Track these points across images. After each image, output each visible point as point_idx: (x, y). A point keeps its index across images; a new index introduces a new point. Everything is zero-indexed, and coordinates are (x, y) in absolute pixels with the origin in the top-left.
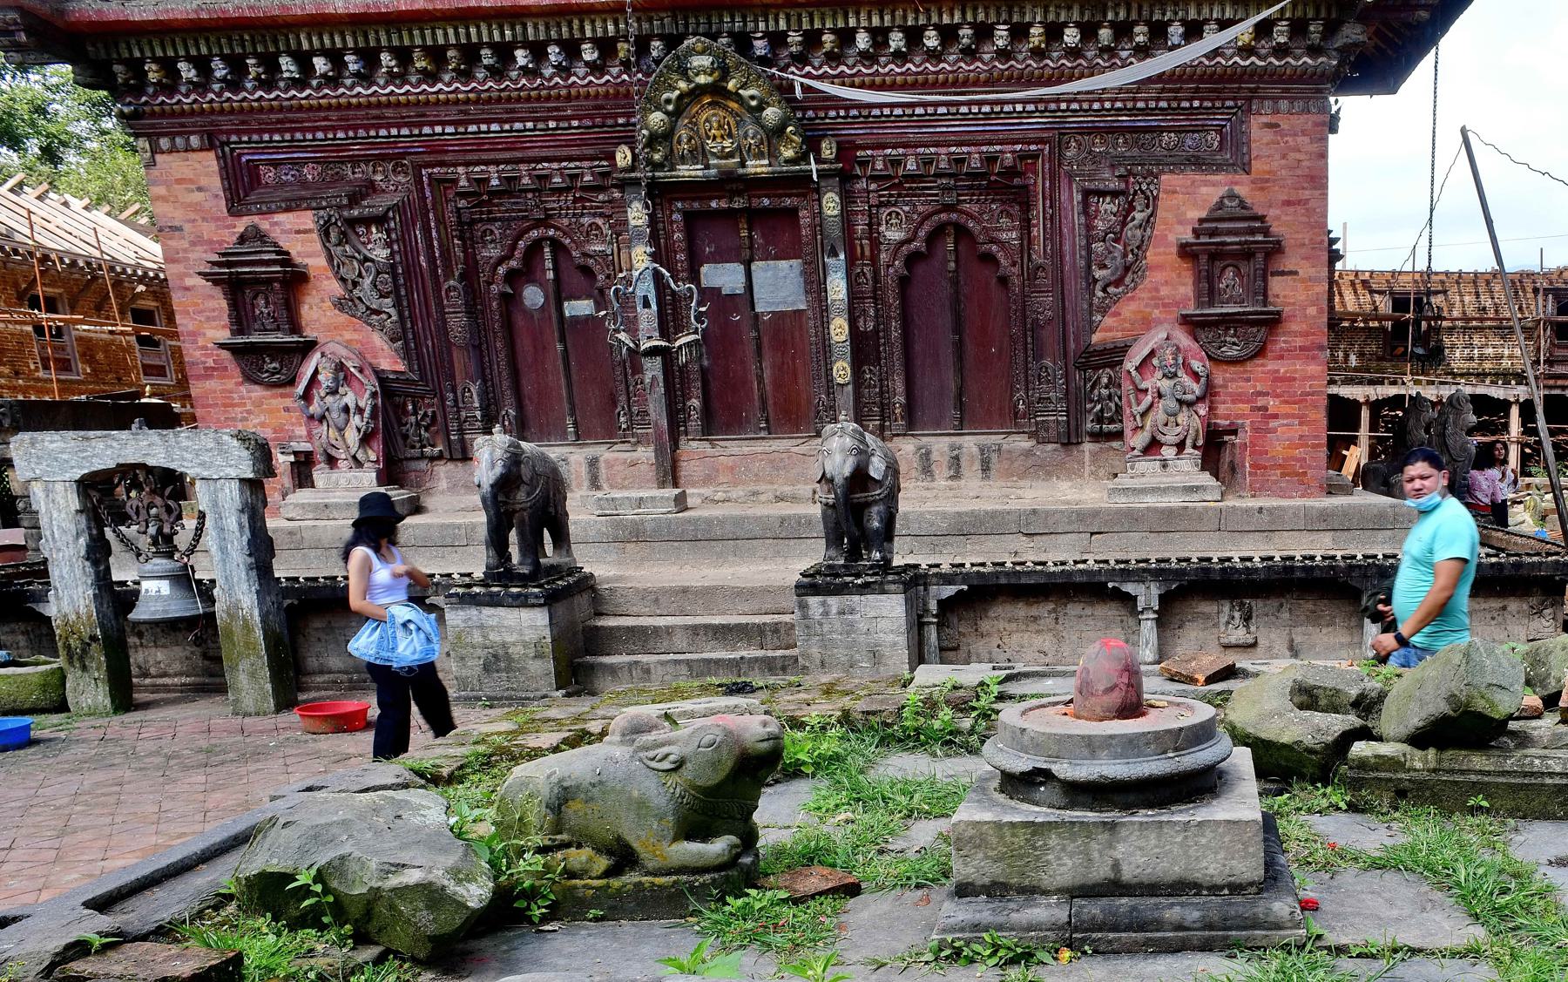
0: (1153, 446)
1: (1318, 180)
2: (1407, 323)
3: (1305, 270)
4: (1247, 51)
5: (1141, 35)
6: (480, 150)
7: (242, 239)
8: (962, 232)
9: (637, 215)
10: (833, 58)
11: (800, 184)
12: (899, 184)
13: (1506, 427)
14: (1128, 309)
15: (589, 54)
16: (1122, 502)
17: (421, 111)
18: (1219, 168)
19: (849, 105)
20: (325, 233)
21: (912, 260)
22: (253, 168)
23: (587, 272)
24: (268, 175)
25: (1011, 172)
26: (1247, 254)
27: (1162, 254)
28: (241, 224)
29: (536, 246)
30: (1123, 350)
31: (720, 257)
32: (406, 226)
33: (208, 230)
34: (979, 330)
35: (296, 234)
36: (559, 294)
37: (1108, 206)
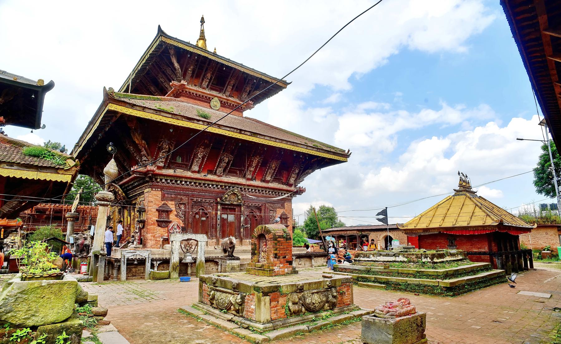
7: (163, 204)
17: (194, 190)
20: (176, 205)
28: (163, 202)
31: (224, 214)
33: (157, 203)
35: (171, 205)
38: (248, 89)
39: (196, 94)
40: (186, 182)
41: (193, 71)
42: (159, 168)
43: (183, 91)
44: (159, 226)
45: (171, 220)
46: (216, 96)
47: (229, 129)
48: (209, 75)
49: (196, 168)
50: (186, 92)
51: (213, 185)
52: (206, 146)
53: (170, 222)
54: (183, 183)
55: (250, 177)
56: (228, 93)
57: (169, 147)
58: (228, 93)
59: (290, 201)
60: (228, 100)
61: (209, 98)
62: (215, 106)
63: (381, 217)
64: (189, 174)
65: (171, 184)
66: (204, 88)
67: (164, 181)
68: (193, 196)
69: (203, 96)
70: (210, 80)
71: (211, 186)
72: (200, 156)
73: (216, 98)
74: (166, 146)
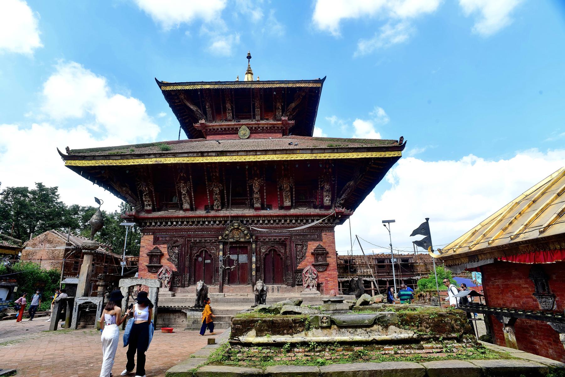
0: (308, 286)
1: (334, 242)
2: (347, 265)
3: (332, 256)
4: (321, 223)
5: (304, 221)
6: (197, 236)
8: (275, 251)
9: (221, 247)
10: (256, 224)
11: (249, 243)
12: (265, 243)
14: (303, 263)
15: (217, 223)
16: (303, 296)
17: (189, 230)
18: (317, 241)
19: (258, 231)
20: (168, 248)
21: (266, 255)
22: (158, 238)
23: (210, 256)
24: (161, 239)
25: (283, 241)
26: (323, 254)
27: (308, 254)
29: (202, 251)
32: (182, 247)
33: (149, 247)
34: (279, 267)
35: (163, 248)
36: (205, 259)
37: (299, 247)
39: (221, 129)
41: (211, 106)
42: (149, 212)
43: (207, 130)
44: (149, 271)
45: (162, 264)
46: (243, 125)
47: (186, 155)
48: (228, 106)
49: (186, 206)
50: (210, 130)
52: (186, 180)
53: (162, 266)
55: (258, 205)
57: (149, 189)
58: (258, 117)
59: (331, 229)
60: (259, 124)
61: (237, 128)
62: (244, 135)
63: (420, 237)
64: (181, 213)
67: (153, 224)
68: (189, 236)
69: (229, 129)
70: (232, 109)
73: (244, 127)
74: (145, 188)
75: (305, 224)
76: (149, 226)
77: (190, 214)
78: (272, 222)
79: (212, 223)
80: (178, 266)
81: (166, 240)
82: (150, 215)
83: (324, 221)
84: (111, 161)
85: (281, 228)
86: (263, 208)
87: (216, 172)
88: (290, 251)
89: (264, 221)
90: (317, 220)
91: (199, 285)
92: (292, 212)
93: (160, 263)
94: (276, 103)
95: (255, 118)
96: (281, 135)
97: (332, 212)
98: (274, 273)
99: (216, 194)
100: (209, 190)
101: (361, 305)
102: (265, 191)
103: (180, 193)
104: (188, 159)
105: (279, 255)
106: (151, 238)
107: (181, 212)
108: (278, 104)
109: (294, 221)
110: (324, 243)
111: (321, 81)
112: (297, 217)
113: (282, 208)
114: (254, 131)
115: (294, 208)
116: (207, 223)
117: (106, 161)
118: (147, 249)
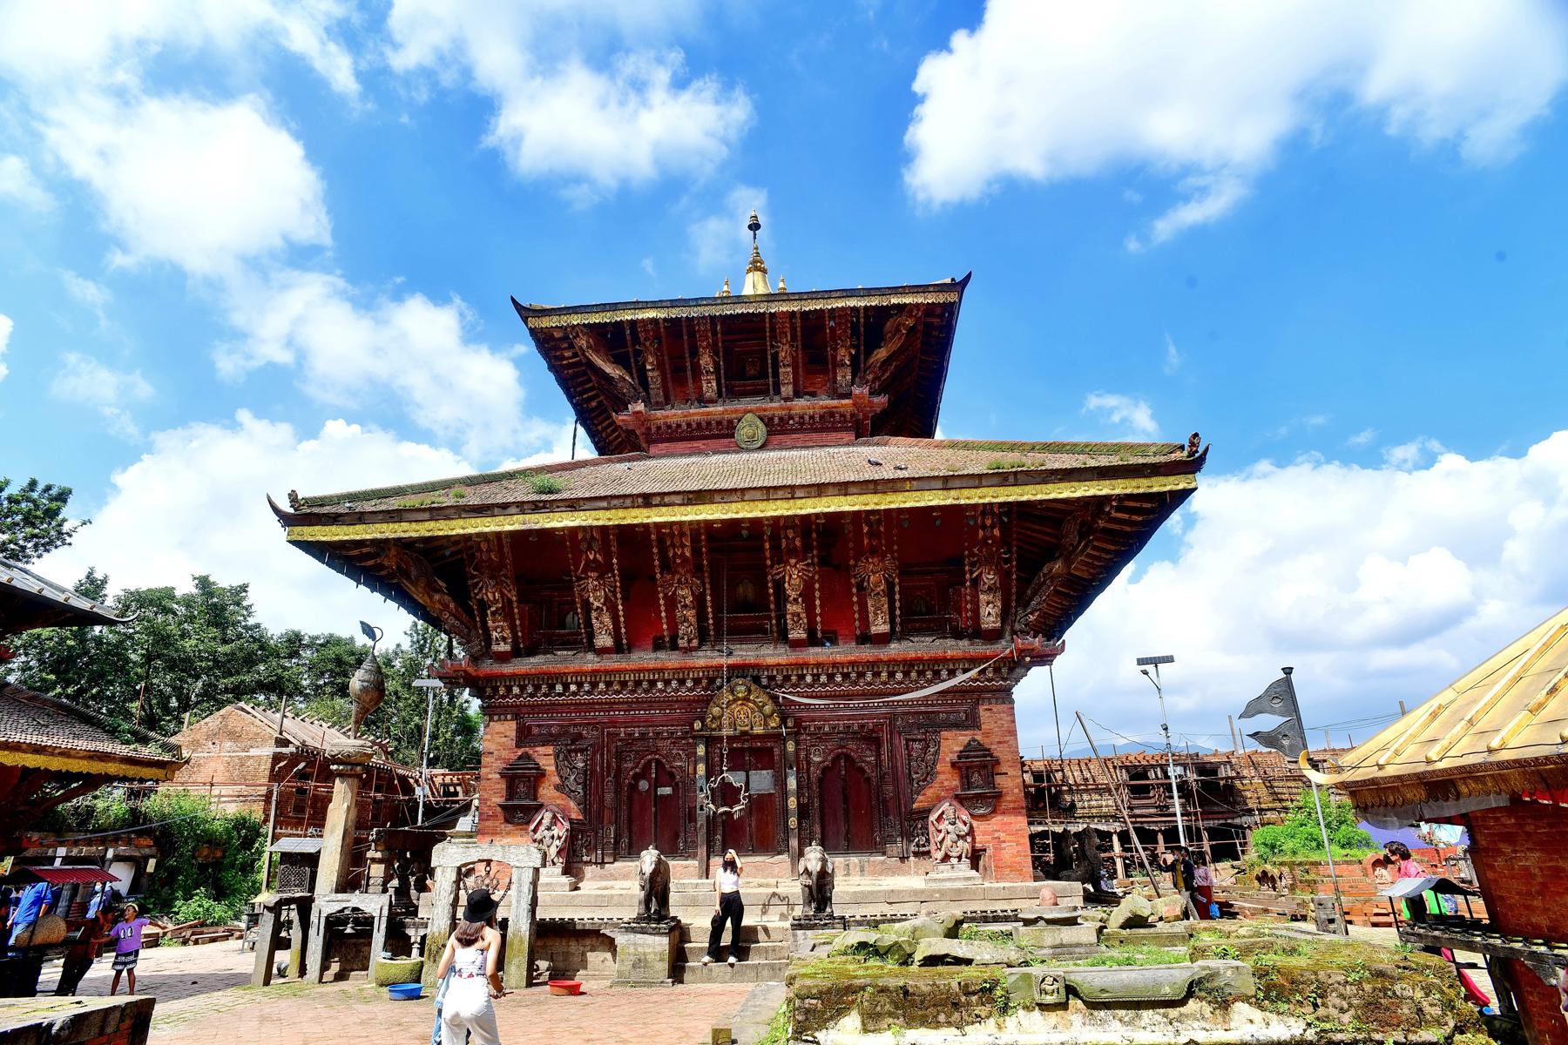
1: (1013, 733)
3: (1011, 772)
4: (971, 680)
5: (929, 675)
6: (633, 723)
7: (520, 758)
8: (848, 757)
9: (701, 750)
10: (794, 686)
11: (777, 737)
12: (819, 737)
13: (1111, 848)
14: (930, 792)
15: (689, 684)
16: (934, 886)
18: (967, 728)
19: (800, 704)
20: (557, 756)
21: (825, 770)
22: (530, 727)
23: (672, 775)
24: (535, 731)
25: (872, 731)
27: (943, 767)
29: (650, 762)
30: (929, 811)
32: (594, 753)
33: (505, 754)
34: (861, 804)
35: (545, 757)
36: (658, 783)
37: (917, 745)
38: (844, 355)
39: (689, 425)
40: (580, 685)
41: (660, 366)
42: (503, 658)
44: (507, 821)
47: (605, 504)
48: (706, 361)
49: (604, 640)
51: (667, 683)
52: (603, 570)
53: (541, 806)
54: (573, 688)
55: (798, 634)
56: (787, 390)
57: (502, 595)
58: (787, 390)
59: (1005, 695)
61: (730, 422)
62: (752, 439)
63: (1269, 722)
64: (590, 662)
65: (540, 699)
66: (712, 401)
67: (516, 690)
68: (613, 723)
69: (709, 423)
71: (660, 685)
72: (596, 604)
75: (930, 682)
76: (503, 697)
77: (612, 662)
78: (839, 679)
79: (674, 684)
80: (585, 804)
81: (551, 735)
82: (507, 669)
83: (983, 672)
84: (405, 525)
85: (864, 695)
86: (813, 640)
87: (683, 546)
88: (892, 758)
89: (816, 677)
90: (965, 671)
91: (649, 858)
92: (895, 649)
93: (535, 799)
94: (835, 349)
95: (778, 392)
96: (850, 436)
97: (1004, 648)
98: (847, 820)
99: (685, 606)
100: (666, 595)
101: (1123, 927)
102: (817, 594)
103: (587, 606)
104: (608, 514)
105: (862, 770)
106: (509, 728)
107: (590, 656)
108: (842, 352)
109: (899, 676)
110: (987, 735)
111: (959, 286)
112: (908, 665)
113: (865, 638)
114: (779, 431)
115: (899, 640)
116: (660, 685)
117: (391, 526)
118: (499, 758)
